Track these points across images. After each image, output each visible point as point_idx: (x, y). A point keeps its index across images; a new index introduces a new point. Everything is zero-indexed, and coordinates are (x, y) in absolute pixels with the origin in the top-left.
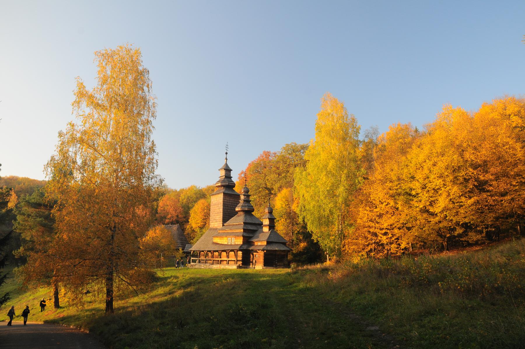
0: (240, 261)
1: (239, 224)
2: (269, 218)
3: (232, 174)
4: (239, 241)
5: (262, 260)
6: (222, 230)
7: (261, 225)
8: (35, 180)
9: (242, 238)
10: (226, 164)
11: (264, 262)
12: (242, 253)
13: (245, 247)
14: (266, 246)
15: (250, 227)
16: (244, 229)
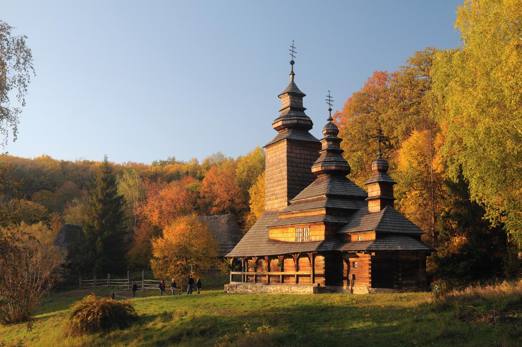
0: (320, 276)
1: (318, 200)
2: (380, 183)
3: (306, 102)
4: (318, 234)
5: (367, 274)
6: (286, 212)
7: (363, 199)
8: (17, 158)
9: (323, 227)
10: (293, 84)
11: (372, 278)
12: (325, 260)
13: (330, 247)
14: (375, 241)
15: (341, 205)
16: (327, 209)
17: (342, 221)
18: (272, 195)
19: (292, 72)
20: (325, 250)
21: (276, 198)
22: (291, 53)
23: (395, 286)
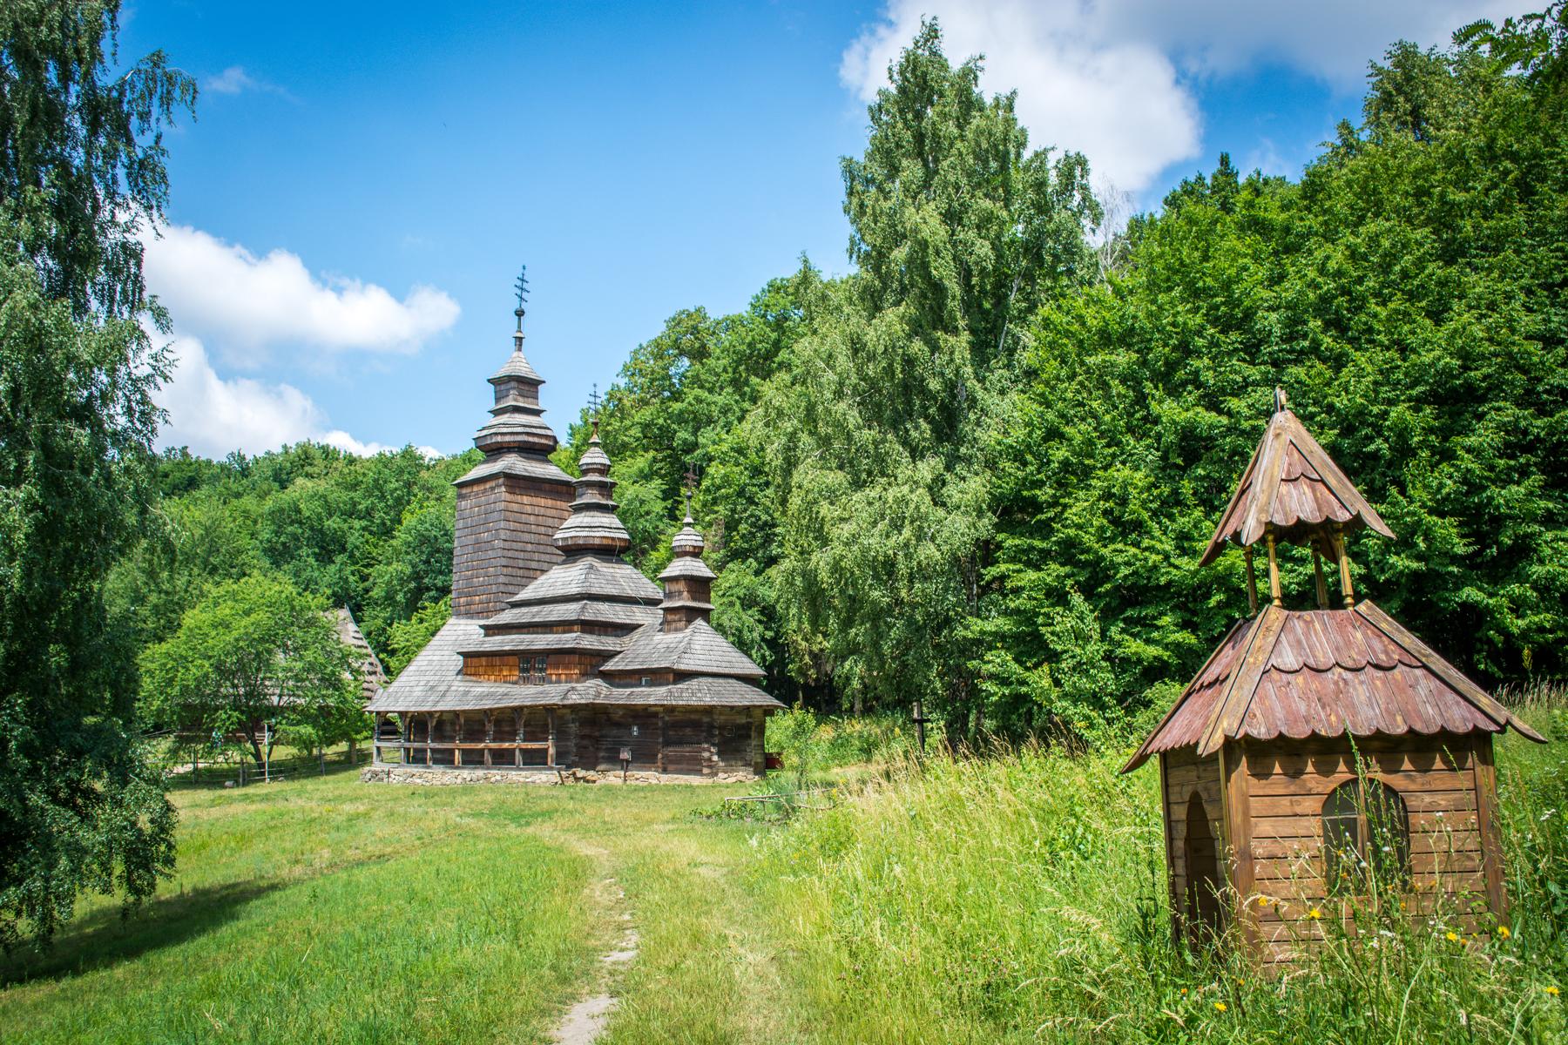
23: (706, 771)
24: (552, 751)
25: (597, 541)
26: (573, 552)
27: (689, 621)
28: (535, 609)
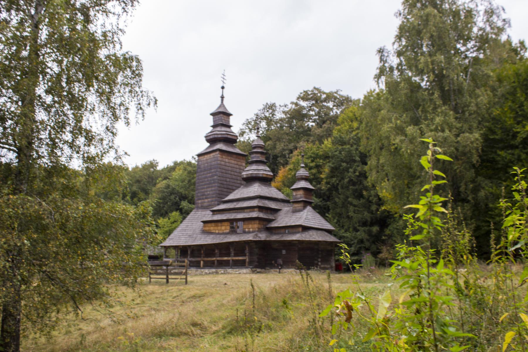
17: (271, 217)
18: (203, 195)
19: (223, 95)
20: (260, 239)
21: (206, 198)
22: (223, 79)
24: (247, 260)
25: (261, 175)
26: (250, 180)
27: (305, 207)
28: (235, 203)
